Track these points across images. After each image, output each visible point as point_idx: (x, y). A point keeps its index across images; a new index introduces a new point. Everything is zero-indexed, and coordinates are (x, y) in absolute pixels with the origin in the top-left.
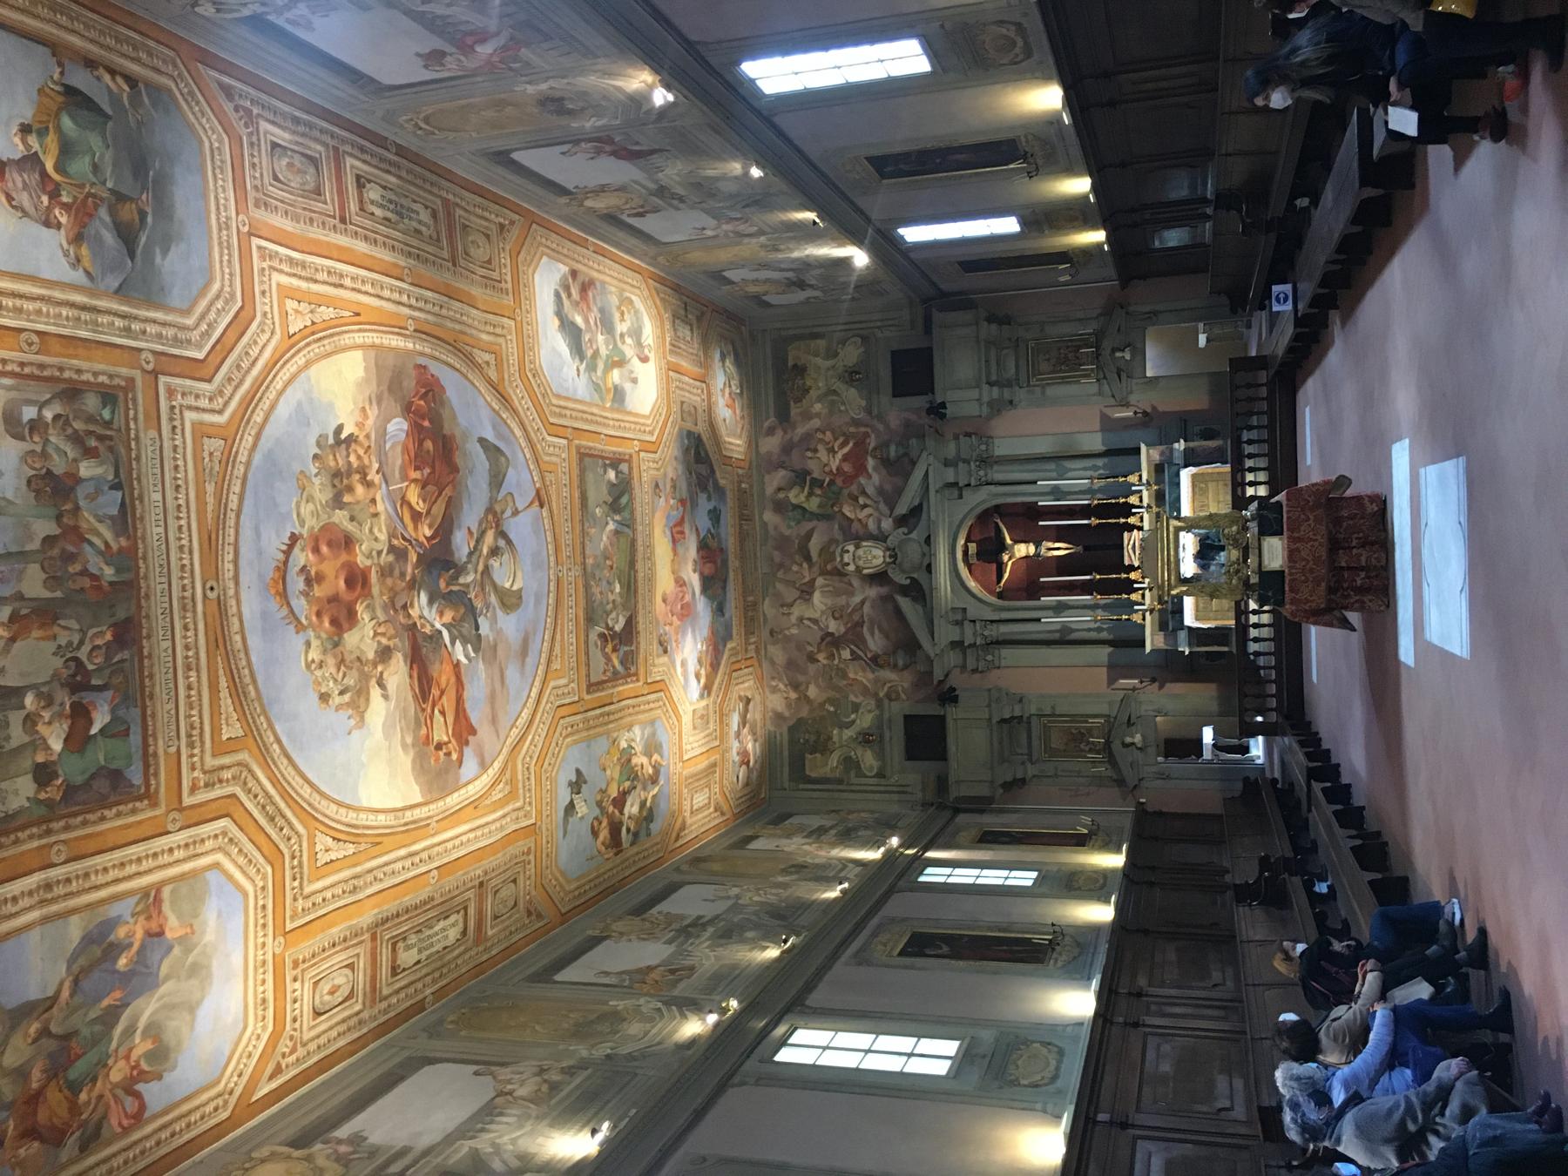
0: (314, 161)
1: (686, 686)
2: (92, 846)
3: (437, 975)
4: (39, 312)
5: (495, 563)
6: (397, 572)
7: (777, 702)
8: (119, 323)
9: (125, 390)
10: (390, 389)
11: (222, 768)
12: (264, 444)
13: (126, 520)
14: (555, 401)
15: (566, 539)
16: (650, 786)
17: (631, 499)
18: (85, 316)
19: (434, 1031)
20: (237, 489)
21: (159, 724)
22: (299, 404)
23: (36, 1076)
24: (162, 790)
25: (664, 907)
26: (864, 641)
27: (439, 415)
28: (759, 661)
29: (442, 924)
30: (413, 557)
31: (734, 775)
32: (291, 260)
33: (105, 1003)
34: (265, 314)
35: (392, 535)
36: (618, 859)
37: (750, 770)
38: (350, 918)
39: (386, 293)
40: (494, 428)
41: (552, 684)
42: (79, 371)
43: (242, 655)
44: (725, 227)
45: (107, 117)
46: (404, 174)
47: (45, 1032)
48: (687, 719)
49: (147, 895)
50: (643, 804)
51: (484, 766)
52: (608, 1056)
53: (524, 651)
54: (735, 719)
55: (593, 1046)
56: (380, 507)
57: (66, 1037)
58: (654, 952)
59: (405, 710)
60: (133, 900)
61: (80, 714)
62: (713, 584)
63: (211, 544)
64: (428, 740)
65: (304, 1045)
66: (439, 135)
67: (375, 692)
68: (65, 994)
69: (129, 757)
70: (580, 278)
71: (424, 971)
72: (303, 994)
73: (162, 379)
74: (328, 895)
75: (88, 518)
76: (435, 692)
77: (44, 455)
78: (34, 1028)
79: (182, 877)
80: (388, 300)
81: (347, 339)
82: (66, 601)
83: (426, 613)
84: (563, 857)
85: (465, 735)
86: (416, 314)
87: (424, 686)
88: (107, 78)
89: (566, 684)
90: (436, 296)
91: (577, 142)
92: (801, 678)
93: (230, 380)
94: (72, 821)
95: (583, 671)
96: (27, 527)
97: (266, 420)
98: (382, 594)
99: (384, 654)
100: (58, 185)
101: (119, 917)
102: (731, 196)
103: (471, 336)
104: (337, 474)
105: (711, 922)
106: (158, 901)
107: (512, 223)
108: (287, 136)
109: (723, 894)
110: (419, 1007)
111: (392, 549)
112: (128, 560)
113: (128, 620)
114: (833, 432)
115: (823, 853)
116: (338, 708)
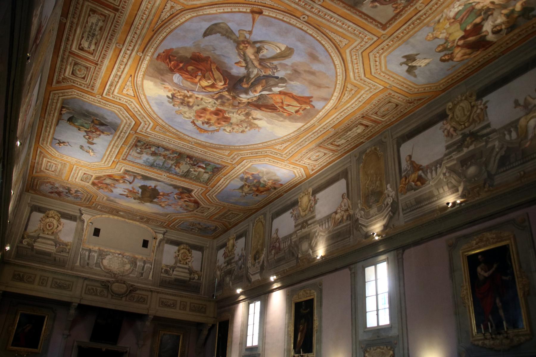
6: (225, 101)
10: (162, 75)
12: (163, 118)
20: (171, 129)
22: (156, 103)
29: (349, 133)
30: (225, 93)
32: (111, 85)
34: (126, 102)
35: (212, 97)
39: (125, 60)
40: (205, 21)
51: (327, 100)
56: (200, 97)
63: (180, 138)
64: (290, 115)
67: (256, 122)
73: (138, 131)
74: (290, 152)
80: (128, 60)
81: (139, 83)
83: (248, 97)
86: (136, 49)
87: (272, 108)
90: (130, 34)
95: (371, 26)
99: (248, 114)
111: (217, 99)
112: (174, 152)
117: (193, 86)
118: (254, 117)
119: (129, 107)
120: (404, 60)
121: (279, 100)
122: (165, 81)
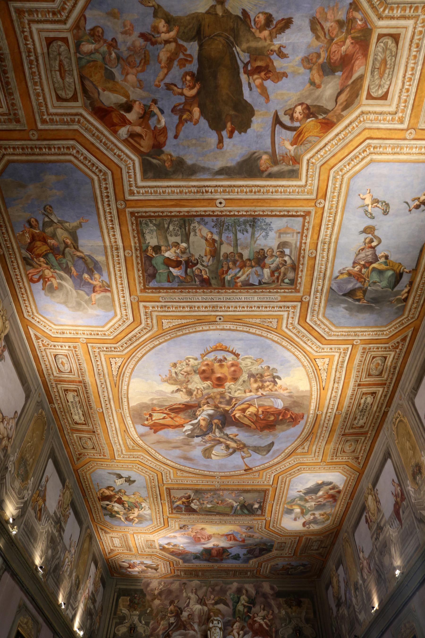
0: (380, 374)
1: (165, 537)
2: (129, 266)
3: (62, 410)
4: (323, 257)
5: (223, 447)
6: (222, 400)
7: (154, 584)
8: (320, 288)
9: (295, 289)
10: (294, 402)
11: (152, 319)
12: (274, 345)
13: (247, 285)
14: (288, 479)
15: (230, 481)
16: (125, 516)
17: (246, 515)
18: (322, 275)
19: (40, 404)
20: (257, 332)
21: (171, 294)
22: (289, 362)
23: (52, 242)
24: (146, 294)
25: (72, 517)
26: (177, 630)
27: (284, 423)
28: (172, 577)
29: (81, 413)
30: (228, 408)
31: (125, 559)
32: (343, 362)
33: (73, 269)
34: (323, 349)
35: (237, 399)
36: (96, 499)
37: (126, 568)
38: (89, 372)
39: (332, 402)
40: (278, 450)
41: (171, 471)
42: (302, 271)
43: (194, 330)
44: (365, 562)
45: (392, 290)
46: (377, 414)
47: (67, 246)
48: (151, 537)
49: (109, 286)
50: (117, 513)
51: (141, 436)
52: (7, 468)
53: (186, 458)
54: (148, 562)
55: (14, 463)
56: (248, 394)
57: (63, 254)
58: (52, 504)
59: (167, 401)
60: (107, 280)
61: (177, 264)
62: (208, 555)
63: (237, 320)
64: (154, 410)
65: (45, 350)
66: (394, 428)
67: (175, 388)
68: (79, 254)
69: (160, 282)
70: (337, 495)
71: (64, 404)
72: (63, 350)
74: (99, 363)
75: (248, 271)
76: (173, 415)
77: (272, 256)
78: (69, 241)
79: (113, 301)
81: (314, 383)
82: (219, 261)
83: (205, 413)
84: (99, 472)
85: (154, 428)
86: (324, 416)
87: (176, 410)
88: (406, 290)
89: (171, 478)
91: (400, 485)
92: (163, 597)
93: (299, 332)
94: (139, 258)
95: (176, 487)
96: (246, 247)
97: (284, 346)
98: (214, 393)
99: (190, 393)
100: (368, 268)
101: (102, 275)
102: (381, 563)
103: (315, 441)
104: (262, 376)
105: (60, 535)
106: (106, 291)
107: (359, 463)
108: (389, 364)
109: (73, 545)
110: (51, 402)
111: (231, 398)
112: (233, 285)
113: (210, 284)
114: (272, 619)
115: (83, 599)
116: (170, 370)
117: (261, 403)
118: (181, 393)
119: (319, 344)
120: (131, 479)
121: (177, 419)
122: (290, 396)
